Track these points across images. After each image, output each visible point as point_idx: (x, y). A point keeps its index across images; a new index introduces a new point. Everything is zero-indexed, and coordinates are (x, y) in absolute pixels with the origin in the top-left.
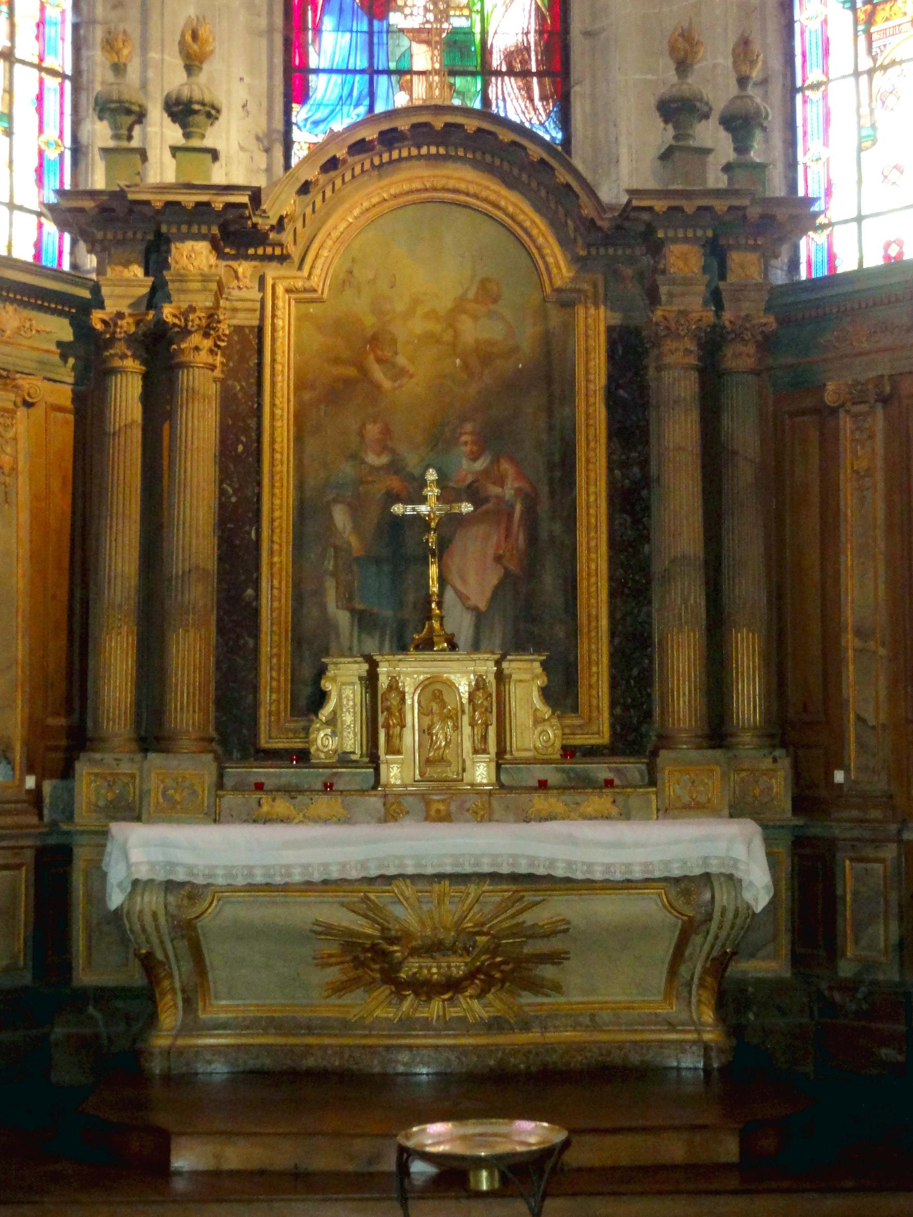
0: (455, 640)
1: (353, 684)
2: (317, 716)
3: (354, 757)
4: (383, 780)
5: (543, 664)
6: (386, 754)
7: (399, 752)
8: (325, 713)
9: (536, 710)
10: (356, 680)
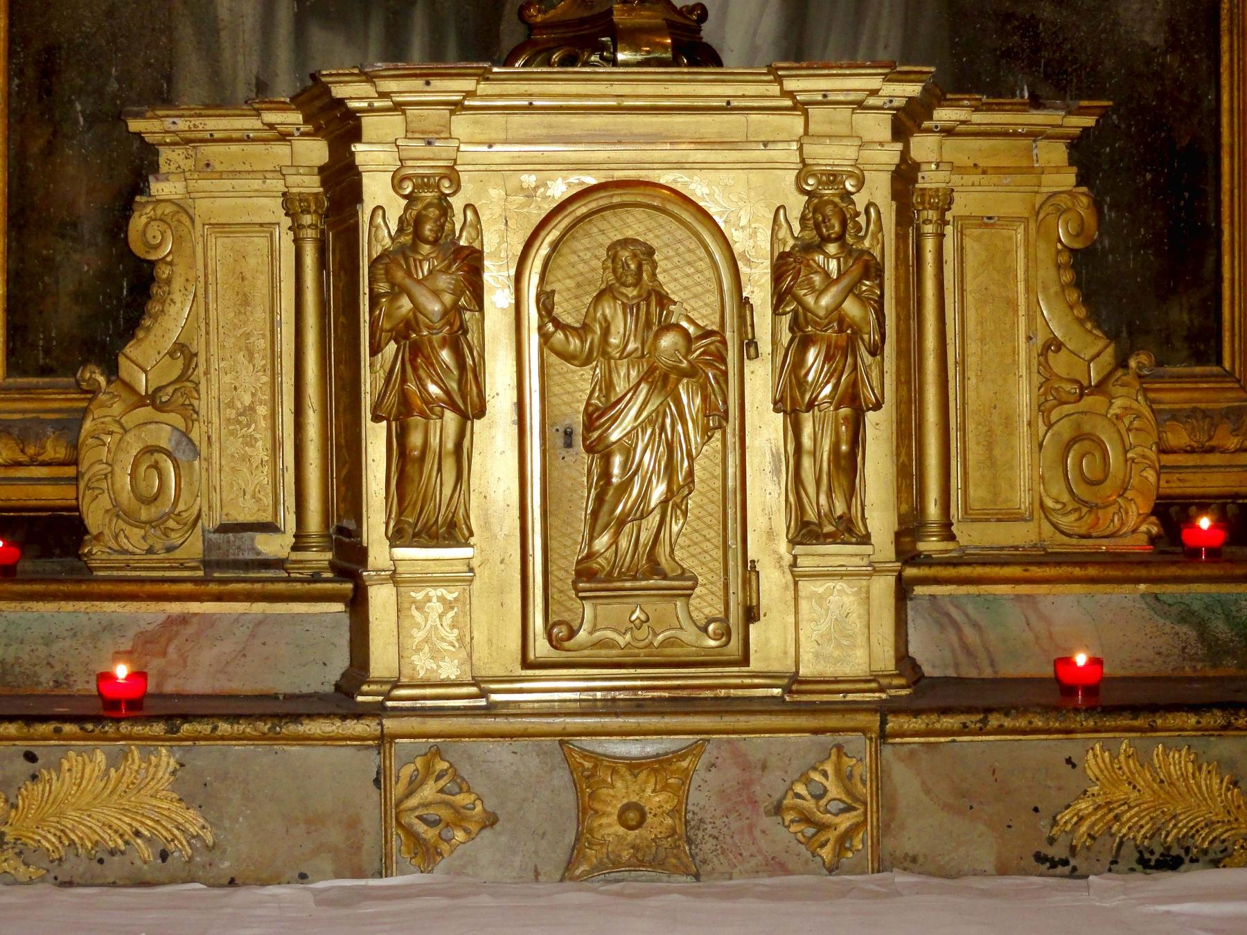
0: (708, 32)
1: (267, 227)
2: (112, 370)
3: (274, 546)
4: (382, 660)
5: (1082, 151)
6: (398, 537)
7: (451, 531)
8: (145, 361)
9: (1053, 345)
10: (273, 209)
